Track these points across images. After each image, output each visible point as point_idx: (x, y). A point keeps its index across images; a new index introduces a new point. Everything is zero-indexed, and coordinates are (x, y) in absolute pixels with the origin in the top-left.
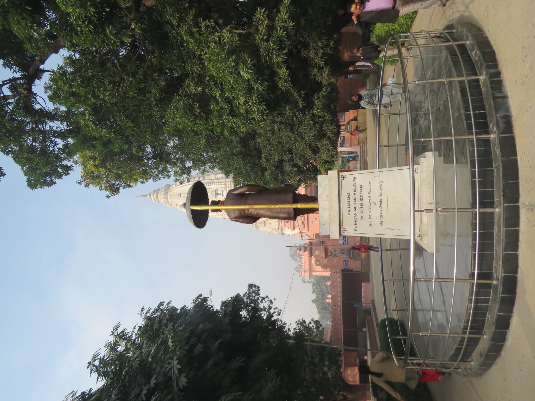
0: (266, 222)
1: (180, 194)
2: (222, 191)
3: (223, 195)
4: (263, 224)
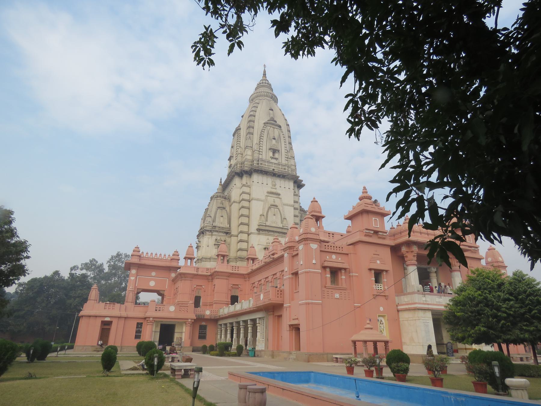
0: (224, 211)
1: (272, 110)
2: (276, 159)
3: (272, 158)
4: (221, 206)
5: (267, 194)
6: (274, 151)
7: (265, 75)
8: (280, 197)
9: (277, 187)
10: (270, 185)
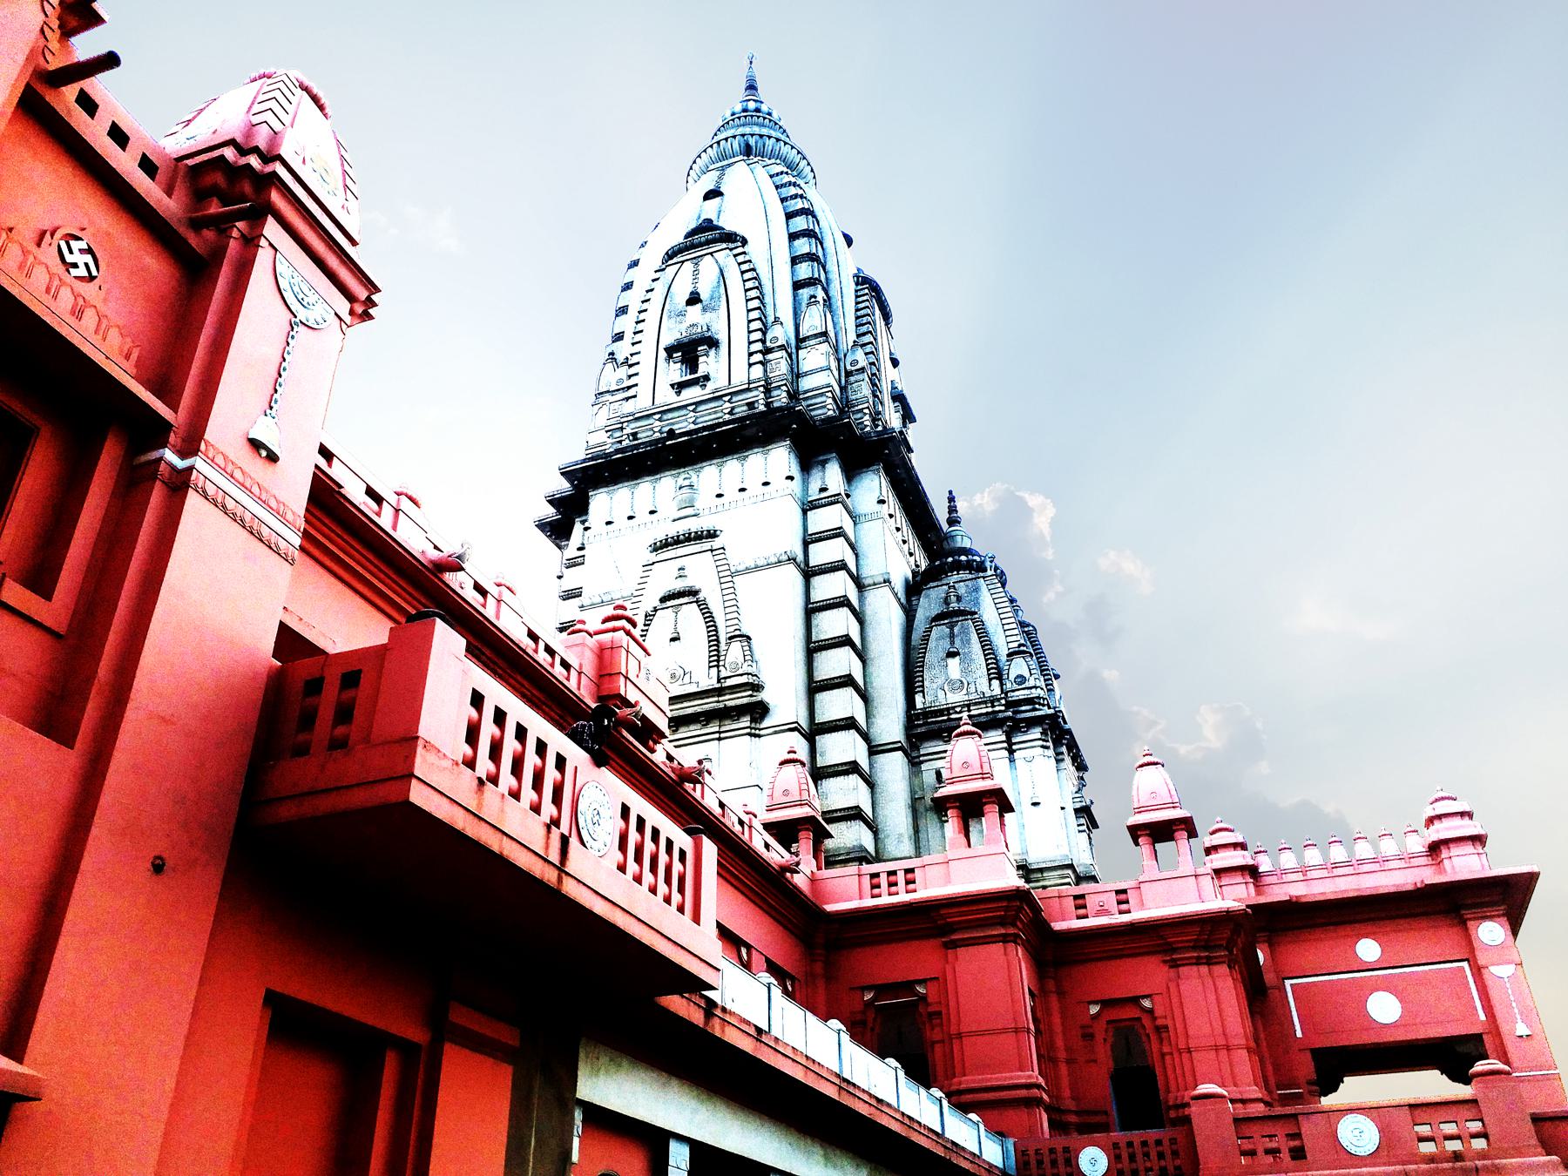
3: (679, 387)
5: (653, 557)
6: (688, 351)
7: (752, 87)
8: (717, 543)
9: (704, 499)
10: (668, 509)
